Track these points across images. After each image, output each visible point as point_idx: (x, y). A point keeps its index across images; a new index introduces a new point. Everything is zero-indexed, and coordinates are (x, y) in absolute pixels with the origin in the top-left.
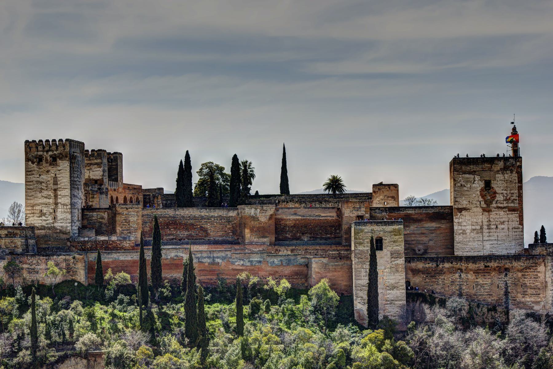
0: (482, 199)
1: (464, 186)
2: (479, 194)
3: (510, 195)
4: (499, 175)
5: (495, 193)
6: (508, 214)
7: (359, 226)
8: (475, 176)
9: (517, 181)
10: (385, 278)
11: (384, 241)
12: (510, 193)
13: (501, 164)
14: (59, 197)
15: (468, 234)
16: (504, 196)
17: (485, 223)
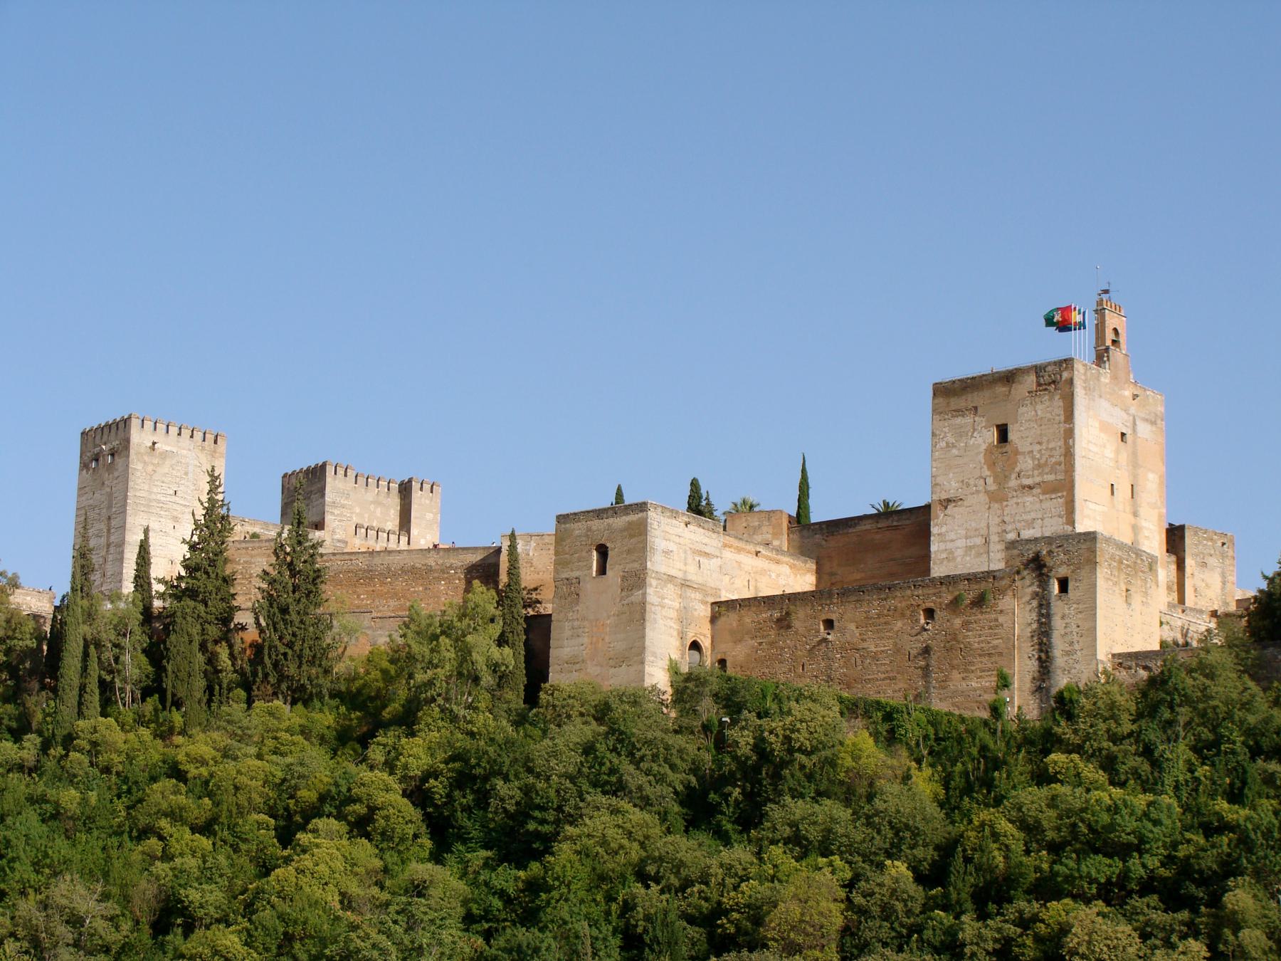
0: (988, 473)
1: (954, 446)
2: (983, 461)
3: (1047, 454)
4: (1024, 409)
5: (1017, 452)
6: (1041, 501)
7: (564, 523)
8: (977, 419)
9: (1062, 418)
10: (607, 639)
11: (610, 553)
12: (1047, 448)
13: (1031, 380)
14: (112, 531)
15: (959, 559)
16: (1033, 458)
17: (993, 529)
